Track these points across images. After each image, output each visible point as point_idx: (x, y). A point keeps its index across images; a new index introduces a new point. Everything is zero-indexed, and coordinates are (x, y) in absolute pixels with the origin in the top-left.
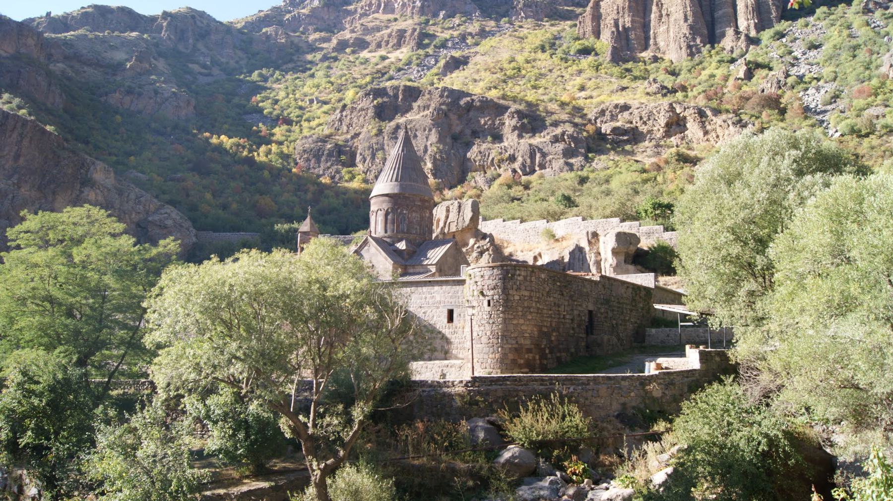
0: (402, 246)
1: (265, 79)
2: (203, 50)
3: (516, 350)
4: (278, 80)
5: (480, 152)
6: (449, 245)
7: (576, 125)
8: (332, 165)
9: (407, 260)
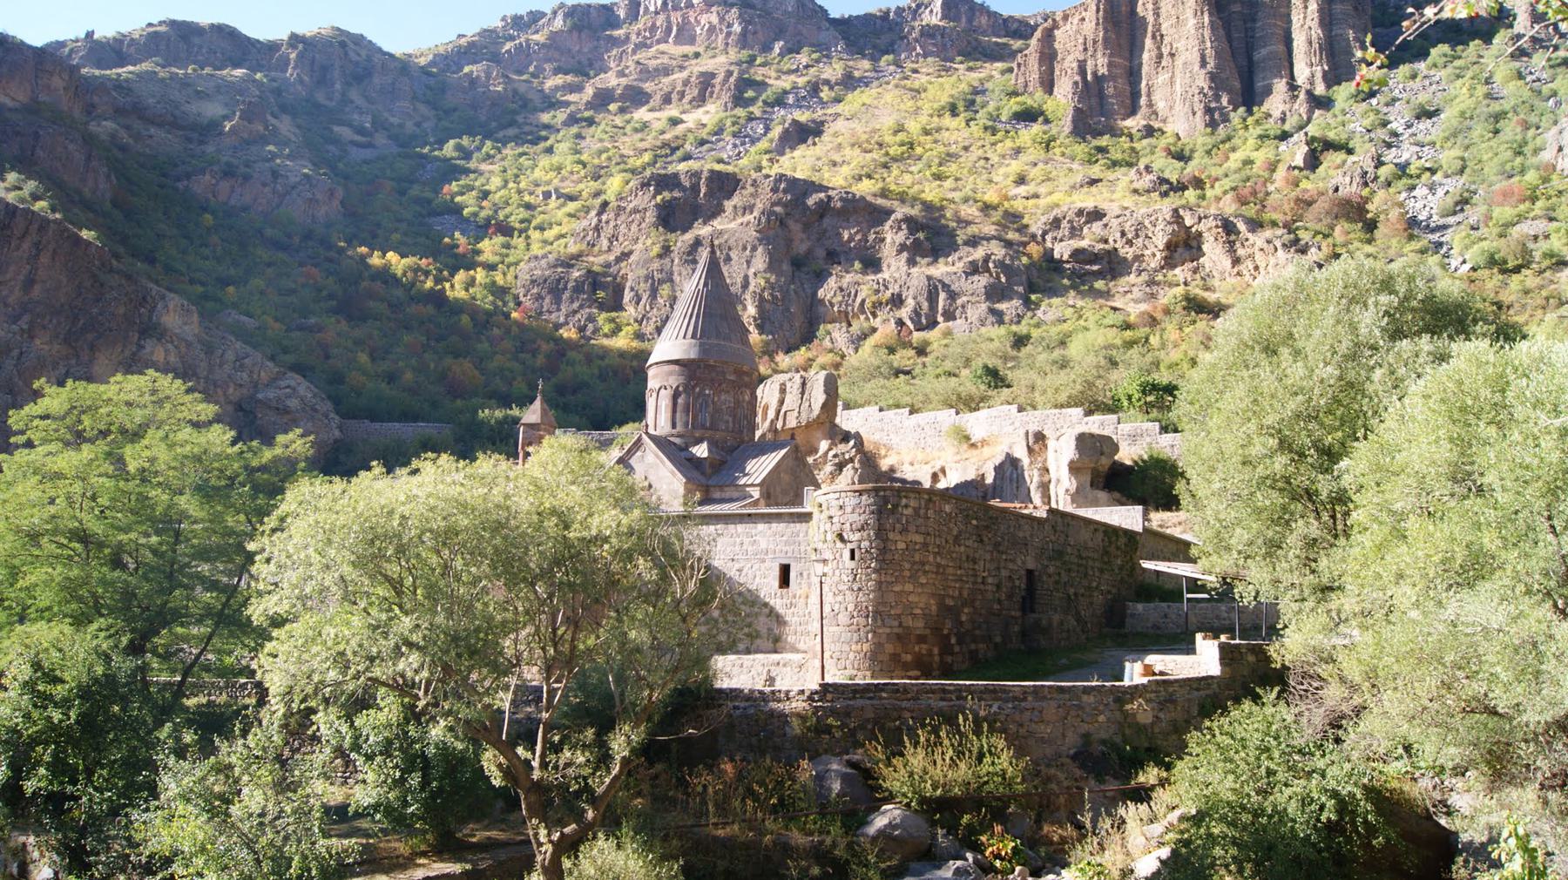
0: (701, 451)
1: (467, 155)
2: (359, 101)
3: (899, 637)
4: (489, 156)
5: (841, 289)
6: (783, 452)
7: (1008, 244)
8: (581, 307)
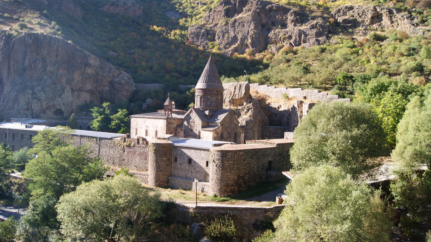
0: (207, 112)
5: (275, 34)
8: (204, 40)
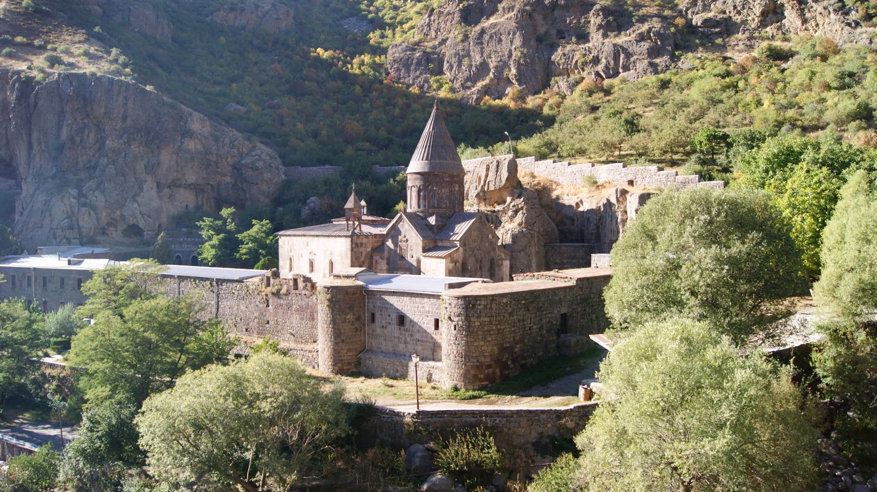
0: (432, 220)
3: (477, 367)
5: (564, 55)
7: (664, 18)
8: (421, 74)
9: (436, 234)
